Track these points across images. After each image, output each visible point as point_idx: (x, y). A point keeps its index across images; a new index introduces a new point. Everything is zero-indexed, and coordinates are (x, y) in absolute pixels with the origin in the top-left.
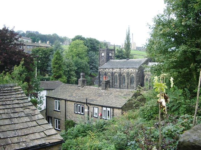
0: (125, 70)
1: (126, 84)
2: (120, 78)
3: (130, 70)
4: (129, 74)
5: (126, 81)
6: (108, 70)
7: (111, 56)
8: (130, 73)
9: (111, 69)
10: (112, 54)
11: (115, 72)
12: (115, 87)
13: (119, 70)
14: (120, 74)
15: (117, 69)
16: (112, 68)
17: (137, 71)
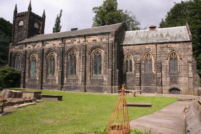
0: (76, 43)
1: (80, 75)
2: (62, 62)
3: (92, 39)
4: (88, 50)
5: (79, 67)
6: (32, 47)
7: (38, 30)
8: (91, 46)
9: (40, 44)
10: (39, 24)
11: (50, 50)
12: (50, 83)
13: (61, 42)
14: (63, 52)
15: (55, 42)
16: (42, 42)
17: (112, 39)
